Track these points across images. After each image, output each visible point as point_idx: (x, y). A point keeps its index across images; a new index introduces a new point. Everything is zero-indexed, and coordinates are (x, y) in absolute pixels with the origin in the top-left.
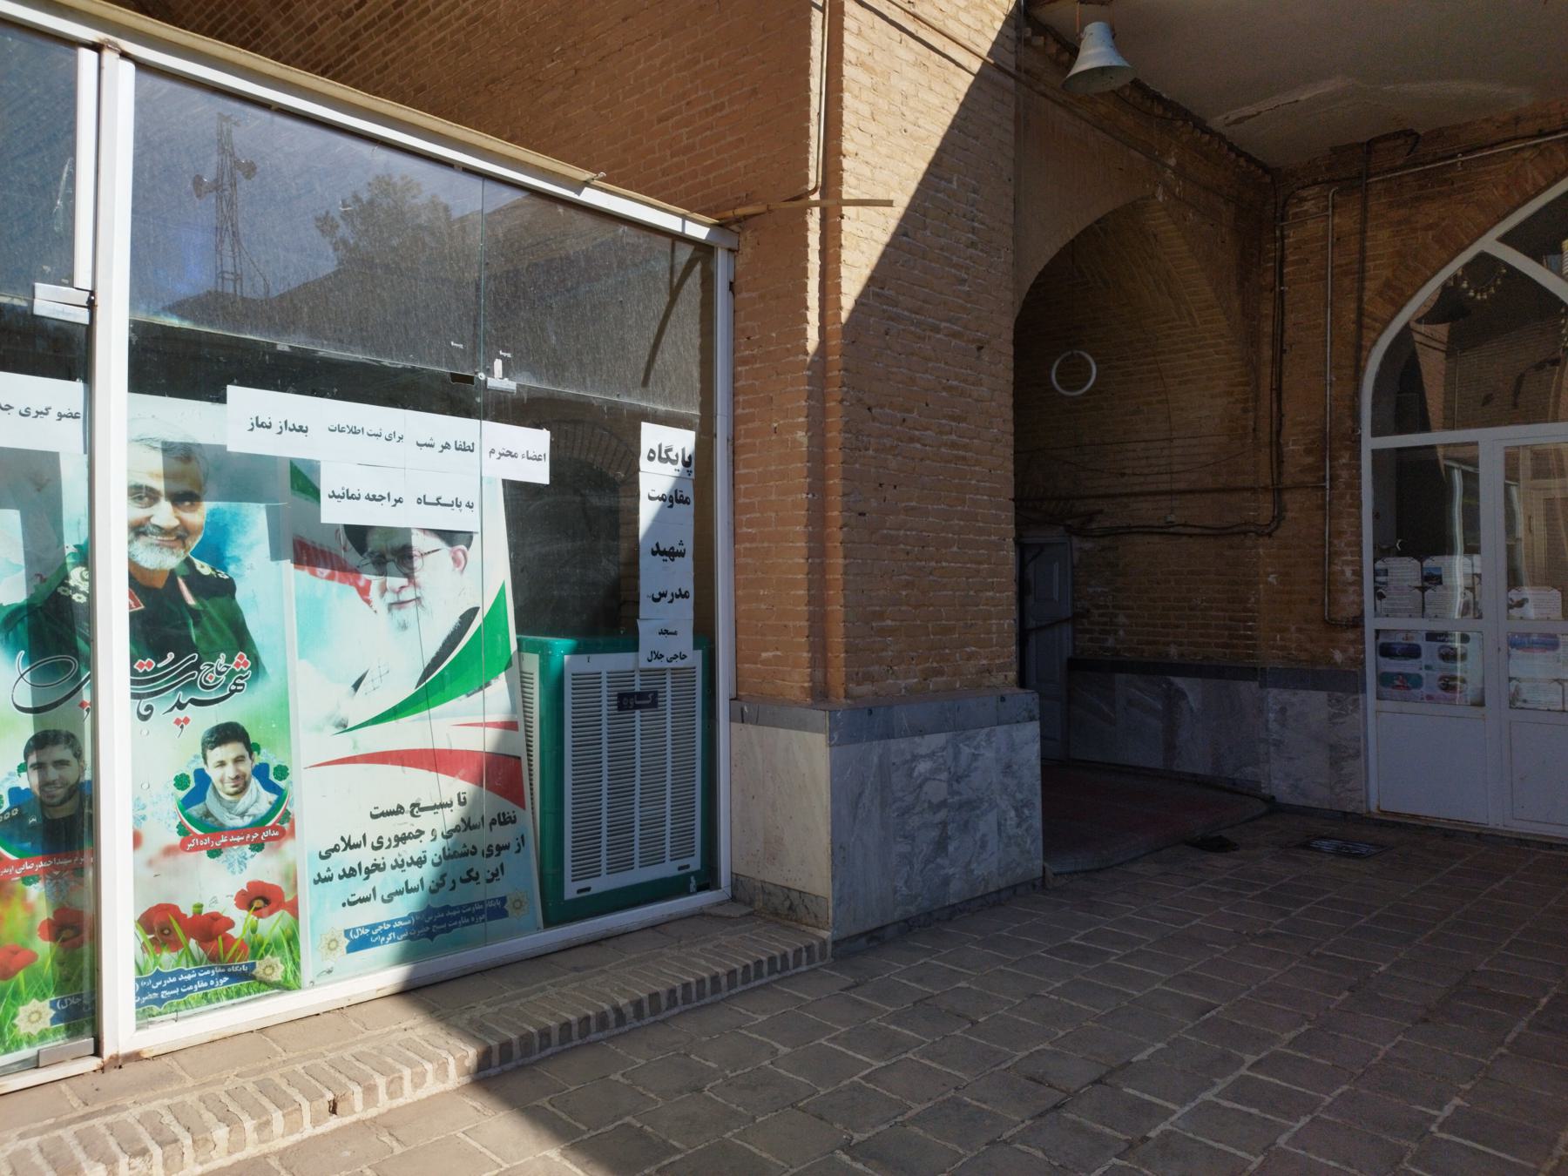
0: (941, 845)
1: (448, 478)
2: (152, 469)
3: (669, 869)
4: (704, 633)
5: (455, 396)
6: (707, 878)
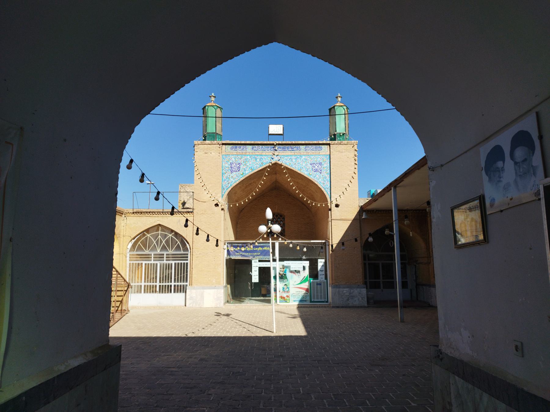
0: (348, 300)
1: (302, 266)
2: (281, 267)
3: (323, 300)
4: (326, 278)
5: (301, 259)
6: (327, 302)
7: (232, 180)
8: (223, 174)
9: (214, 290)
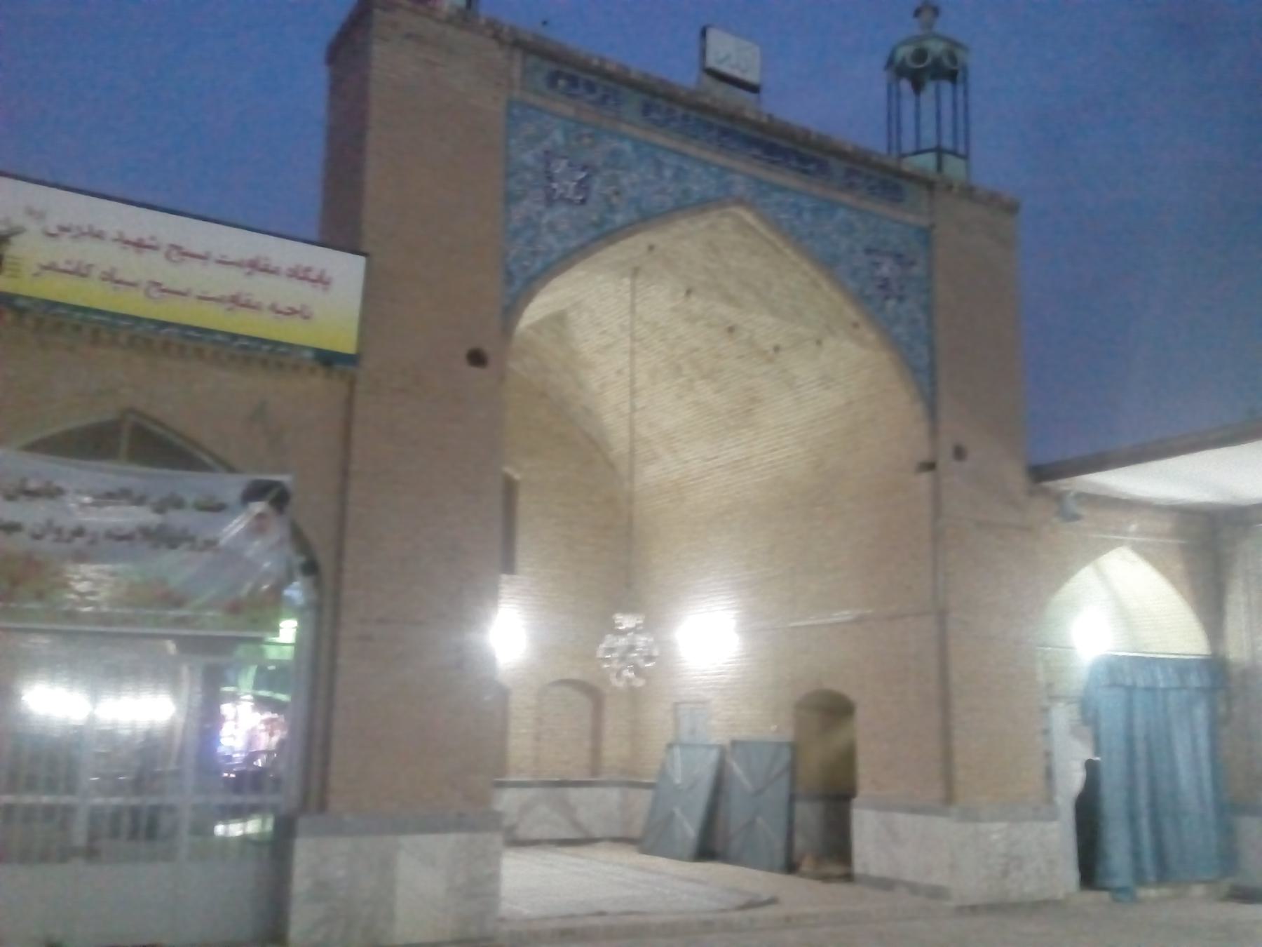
0: (1005, 874)
7: (550, 239)
8: (510, 199)
9: (452, 838)
